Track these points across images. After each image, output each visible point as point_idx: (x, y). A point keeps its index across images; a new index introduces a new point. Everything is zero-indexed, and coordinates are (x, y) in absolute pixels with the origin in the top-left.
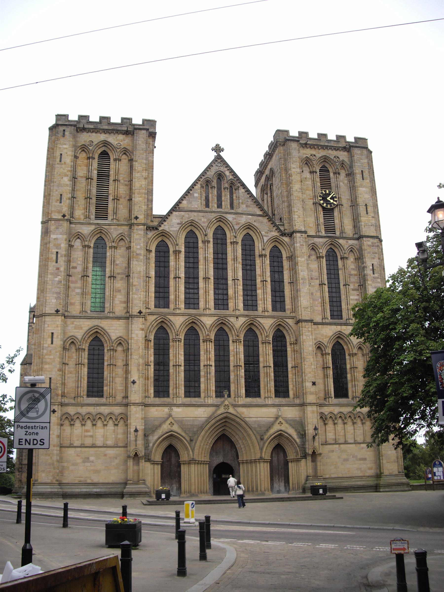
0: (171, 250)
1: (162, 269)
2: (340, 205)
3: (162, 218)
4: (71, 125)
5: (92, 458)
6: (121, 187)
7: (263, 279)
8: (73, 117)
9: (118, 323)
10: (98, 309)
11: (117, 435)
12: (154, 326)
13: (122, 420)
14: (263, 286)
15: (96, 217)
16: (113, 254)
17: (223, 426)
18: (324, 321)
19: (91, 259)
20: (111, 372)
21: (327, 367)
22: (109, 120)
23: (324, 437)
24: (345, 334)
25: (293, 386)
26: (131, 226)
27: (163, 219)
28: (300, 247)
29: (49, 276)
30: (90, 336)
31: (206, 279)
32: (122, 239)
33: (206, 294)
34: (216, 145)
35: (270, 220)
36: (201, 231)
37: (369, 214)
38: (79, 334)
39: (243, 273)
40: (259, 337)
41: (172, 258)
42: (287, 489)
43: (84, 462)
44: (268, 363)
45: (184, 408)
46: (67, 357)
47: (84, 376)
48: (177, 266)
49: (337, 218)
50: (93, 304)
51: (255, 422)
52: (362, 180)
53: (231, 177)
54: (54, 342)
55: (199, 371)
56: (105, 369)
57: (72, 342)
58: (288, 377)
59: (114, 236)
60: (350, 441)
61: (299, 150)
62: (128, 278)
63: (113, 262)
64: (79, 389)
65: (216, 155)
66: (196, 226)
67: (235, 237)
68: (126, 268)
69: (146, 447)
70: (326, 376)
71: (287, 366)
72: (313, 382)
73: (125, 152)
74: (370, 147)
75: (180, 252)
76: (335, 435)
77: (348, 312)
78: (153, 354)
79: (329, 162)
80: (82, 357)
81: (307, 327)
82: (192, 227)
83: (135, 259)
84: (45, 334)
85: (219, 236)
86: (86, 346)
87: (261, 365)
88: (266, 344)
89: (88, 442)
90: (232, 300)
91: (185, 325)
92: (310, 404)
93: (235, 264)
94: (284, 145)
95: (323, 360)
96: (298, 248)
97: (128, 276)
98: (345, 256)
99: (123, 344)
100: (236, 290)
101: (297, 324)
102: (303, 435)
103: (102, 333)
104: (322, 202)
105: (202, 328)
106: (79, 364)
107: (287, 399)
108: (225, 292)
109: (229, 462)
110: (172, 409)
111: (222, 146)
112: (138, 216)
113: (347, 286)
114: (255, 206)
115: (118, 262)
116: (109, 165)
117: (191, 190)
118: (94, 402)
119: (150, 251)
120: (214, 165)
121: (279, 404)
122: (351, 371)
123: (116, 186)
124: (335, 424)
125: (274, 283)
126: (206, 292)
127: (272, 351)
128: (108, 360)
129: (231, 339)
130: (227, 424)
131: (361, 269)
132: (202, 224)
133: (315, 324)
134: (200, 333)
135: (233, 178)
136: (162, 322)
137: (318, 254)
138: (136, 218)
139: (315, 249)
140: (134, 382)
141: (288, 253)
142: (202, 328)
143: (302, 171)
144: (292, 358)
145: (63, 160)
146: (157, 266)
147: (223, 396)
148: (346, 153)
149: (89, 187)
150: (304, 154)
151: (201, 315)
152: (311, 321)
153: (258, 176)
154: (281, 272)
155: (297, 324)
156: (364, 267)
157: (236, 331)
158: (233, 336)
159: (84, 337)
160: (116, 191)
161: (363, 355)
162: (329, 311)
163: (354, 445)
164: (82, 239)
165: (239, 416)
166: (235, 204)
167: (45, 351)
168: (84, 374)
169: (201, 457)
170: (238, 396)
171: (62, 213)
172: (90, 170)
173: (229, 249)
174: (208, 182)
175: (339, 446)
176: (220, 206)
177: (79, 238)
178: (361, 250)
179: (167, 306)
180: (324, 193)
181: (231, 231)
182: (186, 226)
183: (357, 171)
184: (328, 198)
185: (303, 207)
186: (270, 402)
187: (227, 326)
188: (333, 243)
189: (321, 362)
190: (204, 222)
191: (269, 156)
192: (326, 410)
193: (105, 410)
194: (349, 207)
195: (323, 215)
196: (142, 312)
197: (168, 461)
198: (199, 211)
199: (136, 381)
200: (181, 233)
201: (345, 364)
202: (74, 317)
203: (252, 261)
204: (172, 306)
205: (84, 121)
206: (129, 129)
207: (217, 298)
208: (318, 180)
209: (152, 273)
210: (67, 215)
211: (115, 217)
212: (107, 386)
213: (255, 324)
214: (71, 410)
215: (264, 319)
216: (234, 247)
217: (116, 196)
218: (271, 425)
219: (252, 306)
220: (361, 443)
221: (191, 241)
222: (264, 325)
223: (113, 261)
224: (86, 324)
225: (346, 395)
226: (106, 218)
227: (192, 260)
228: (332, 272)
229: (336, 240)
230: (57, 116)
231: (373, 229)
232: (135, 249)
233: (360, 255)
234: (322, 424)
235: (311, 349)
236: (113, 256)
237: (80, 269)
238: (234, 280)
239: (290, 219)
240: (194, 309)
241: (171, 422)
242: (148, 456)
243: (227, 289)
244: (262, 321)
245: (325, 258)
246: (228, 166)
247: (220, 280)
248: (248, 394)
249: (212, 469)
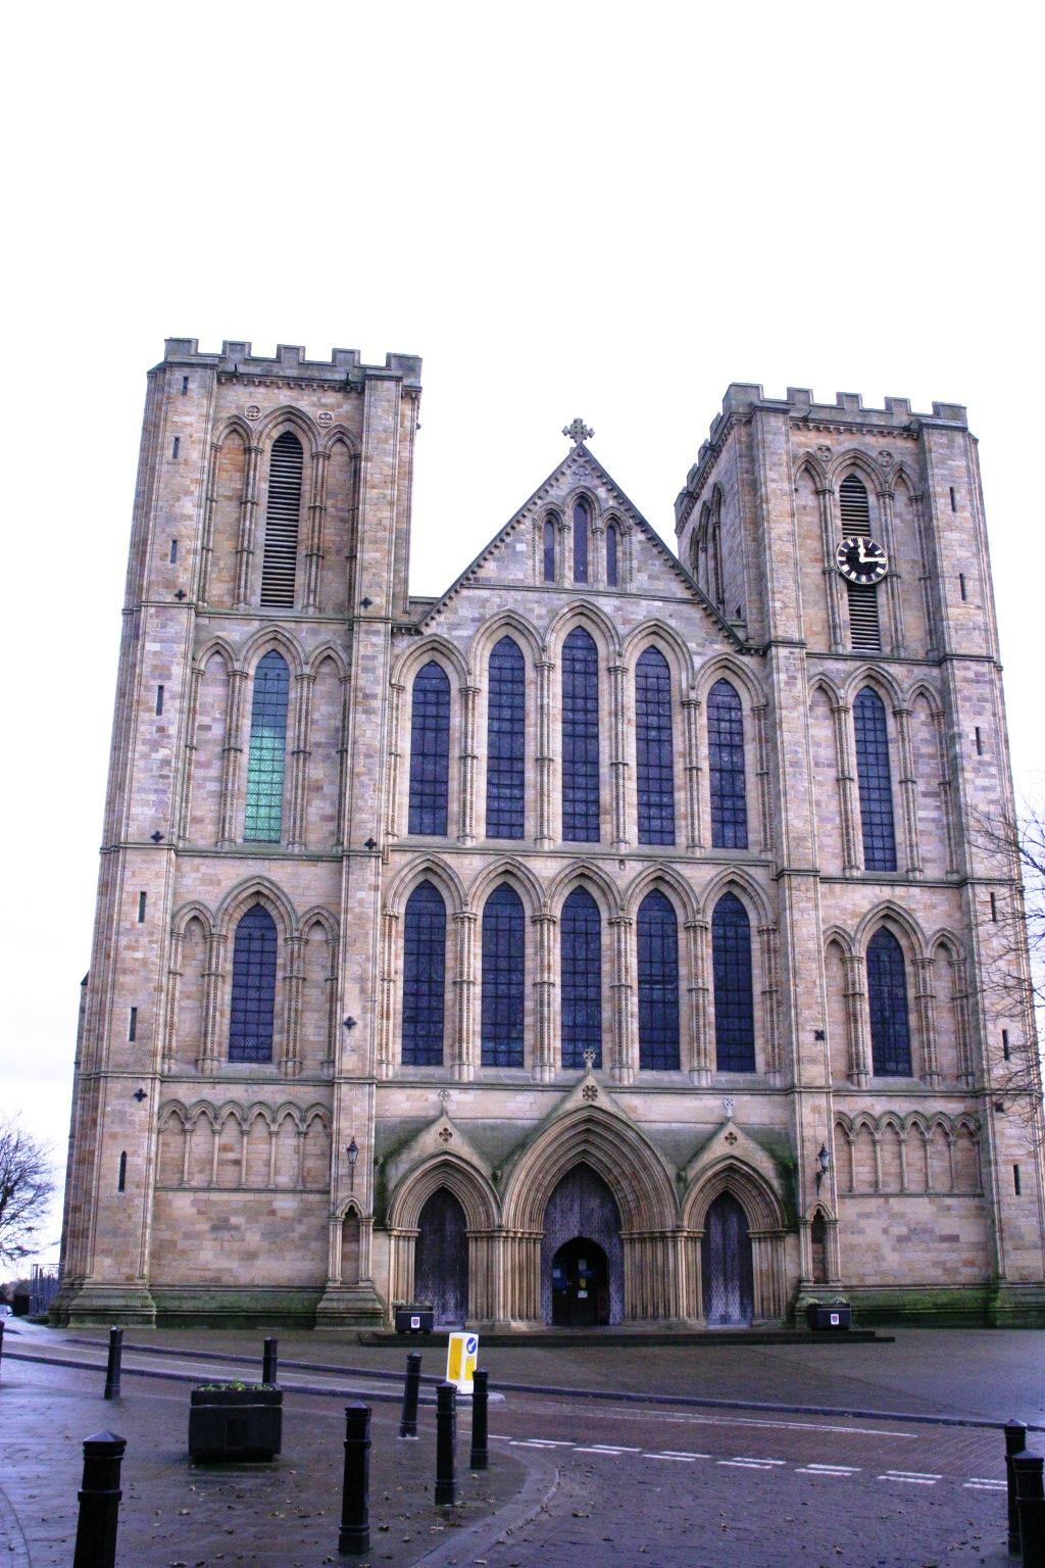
0: (455, 686)
1: (430, 735)
2: (892, 576)
3: (431, 604)
4: (205, 366)
6: (328, 525)
7: (691, 762)
8: (210, 346)
9: (313, 870)
10: (263, 836)
11: (304, 1159)
12: (407, 880)
13: (317, 1120)
14: (691, 781)
15: (262, 601)
16: (305, 694)
17: (579, 1144)
18: (848, 875)
19: (249, 707)
20: (294, 996)
21: (854, 995)
22: (301, 353)
23: (845, 1177)
24: (900, 907)
25: (767, 1042)
26: (350, 624)
27: (433, 607)
28: (787, 684)
29: (141, 748)
30: (241, 903)
31: (542, 761)
32: (329, 657)
33: (542, 800)
34: (575, 422)
35: (709, 612)
36: (530, 638)
37: (969, 599)
38: (211, 898)
39: (638, 748)
40: (680, 912)
41: (456, 709)
42: (749, 1315)
43: (215, 1228)
44: (700, 981)
45: (480, 1092)
46: (180, 957)
47: (222, 1005)
48: (470, 728)
49: (886, 609)
50: (250, 823)
51: (666, 1132)
52: (950, 512)
53: (612, 503)
54: (147, 917)
55: (521, 998)
56: (277, 989)
57: (195, 918)
58: (751, 1017)
59: (309, 649)
60: (913, 1188)
61: (787, 436)
62: (342, 758)
63: (305, 716)
64: (209, 1039)
65: (575, 445)
66: (520, 627)
67: (620, 655)
68: (337, 730)
69: (382, 1195)
70: (851, 1017)
71: (750, 989)
72: (817, 1032)
73: (342, 436)
75: (477, 691)
76: (876, 1172)
77: (911, 851)
78: (401, 952)
79: (865, 467)
80: (218, 957)
81: (803, 888)
82: (510, 628)
83: (360, 709)
84: (124, 896)
85: (580, 654)
86: (229, 929)
87: (683, 986)
88: (695, 932)
89: (229, 1175)
90: (608, 817)
91: (486, 881)
92: (813, 1090)
93: (620, 725)
94: (749, 422)
95: (846, 975)
96: (782, 685)
97: (343, 752)
98: (905, 706)
99: (326, 925)
100: (621, 791)
101: (777, 880)
102: (788, 1170)
103: (272, 896)
104: (846, 568)
105: (529, 886)
106: (209, 975)
107: (749, 1076)
108: (592, 797)
109: (595, 1237)
110: (449, 1095)
111: (589, 424)
112: (372, 599)
113: (910, 784)
114: (673, 576)
115: (316, 715)
116: (300, 468)
117: (508, 534)
118: (246, 1075)
119: (401, 689)
120: (568, 472)
121: (725, 1087)
122: (918, 1005)
123: (317, 523)
124: (874, 1143)
125: (718, 775)
126: (542, 794)
127: (710, 951)
128: (285, 966)
129: (604, 915)
130: (592, 1138)
131: (947, 739)
132: (535, 622)
133: (825, 880)
134: (525, 899)
135: (616, 505)
136: (427, 869)
137: (834, 700)
138: (366, 603)
139: (827, 688)
140: (350, 1024)
141: (755, 699)
142: (529, 886)
143: (796, 490)
144: (762, 968)
145: (181, 453)
146: (419, 730)
147: (583, 1065)
148: (910, 444)
149: (248, 523)
150: (800, 445)
151: (527, 854)
152: (814, 873)
153: (683, 507)
154: (737, 748)
155: (777, 880)
156: (953, 737)
157: (617, 896)
158: (610, 908)
159: (225, 906)
160: (316, 534)
161: (950, 964)
162: (861, 849)
163: (926, 1200)
164: (225, 655)
165: (623, 1116)
167: (123, 941)
168: (223, 999)
169: (522, 1226)
170: (620, 1064)
171: (175, 587)
172: (251, 480)
173: (604, 685)
174: (553, 517)
175: (887, 1202)
176: (581, 575)
177: (218, 652)
178: (945, 691)
179: (440, 829)
180: (852, 545)
181: (610, 640)
182: (495, 626)
183: (939, 488)
184: (863, 559)
185: (796, 582)
186: (705, 1081)
187: (595, 882)
188: (873, 673)
189: (840, 982)
190: (540, 617)
191: (710, 452)
193: (272, 1094)
194: (917, 582)
195: (847, 603)
196: (375, 844)
197: (435, 1232)
198: (528, 589)
199: (356, 1019)
200: (481, 643)
201: (904, 986)
202: (202, 854)
203: (662, 718)
204: (453, 829)
205: (237, 356)
206: (350, 378)
207: (570, 810)
208: (837, 512)
209: (405, 745)
210: (188, 592)
211: (311, 602)
212: (281, 1032)
213: (668, 878)
214: (186, 1094)
215: (690, 866)
216: (616, 681)
217: (315, 547)
218: (703, 1143)
219: (662, 832)
220: (944, 1195)
221: (508, 665)
222: (691, 881)
223: (304, 711)
224: (232, 874)
226: (291, 604)
227: (507, 713)
228: (871, 748)
229: (882, 665)
230: (169, 341)
231: (977, 636)
232: (361, 683)
233: (943, 701)
234: (842, 1141)
235: (812, 945)
236: (304, 699)
237: (218, 730)
238: (616, 764)
239: (763, 613)
240: (511, 837)
241: (446, 1130)
242: (383, 1218)
243: (597, 789)
244: (685, 871)
245: (851, 712)
246: (602, 474)
247: (577, 766)
248: (648, 1061)
249: (552, 1256)
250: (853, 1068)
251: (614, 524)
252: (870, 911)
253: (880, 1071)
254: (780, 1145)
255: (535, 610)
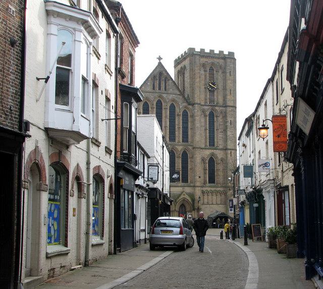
70: (205, 173)
74: (235, 57)
102: (193, 200)
166: (167, 89)
174: (155, 77)
176: (160, 89)
186: (180, 185)
192: (204, 189)
208: (208, 75)
218: (180, 195)
225: (214, 182)
239: (193, 97)
250: (205, 183)
251: (166, 78)
254: (192, 196)
255: (151, 97)
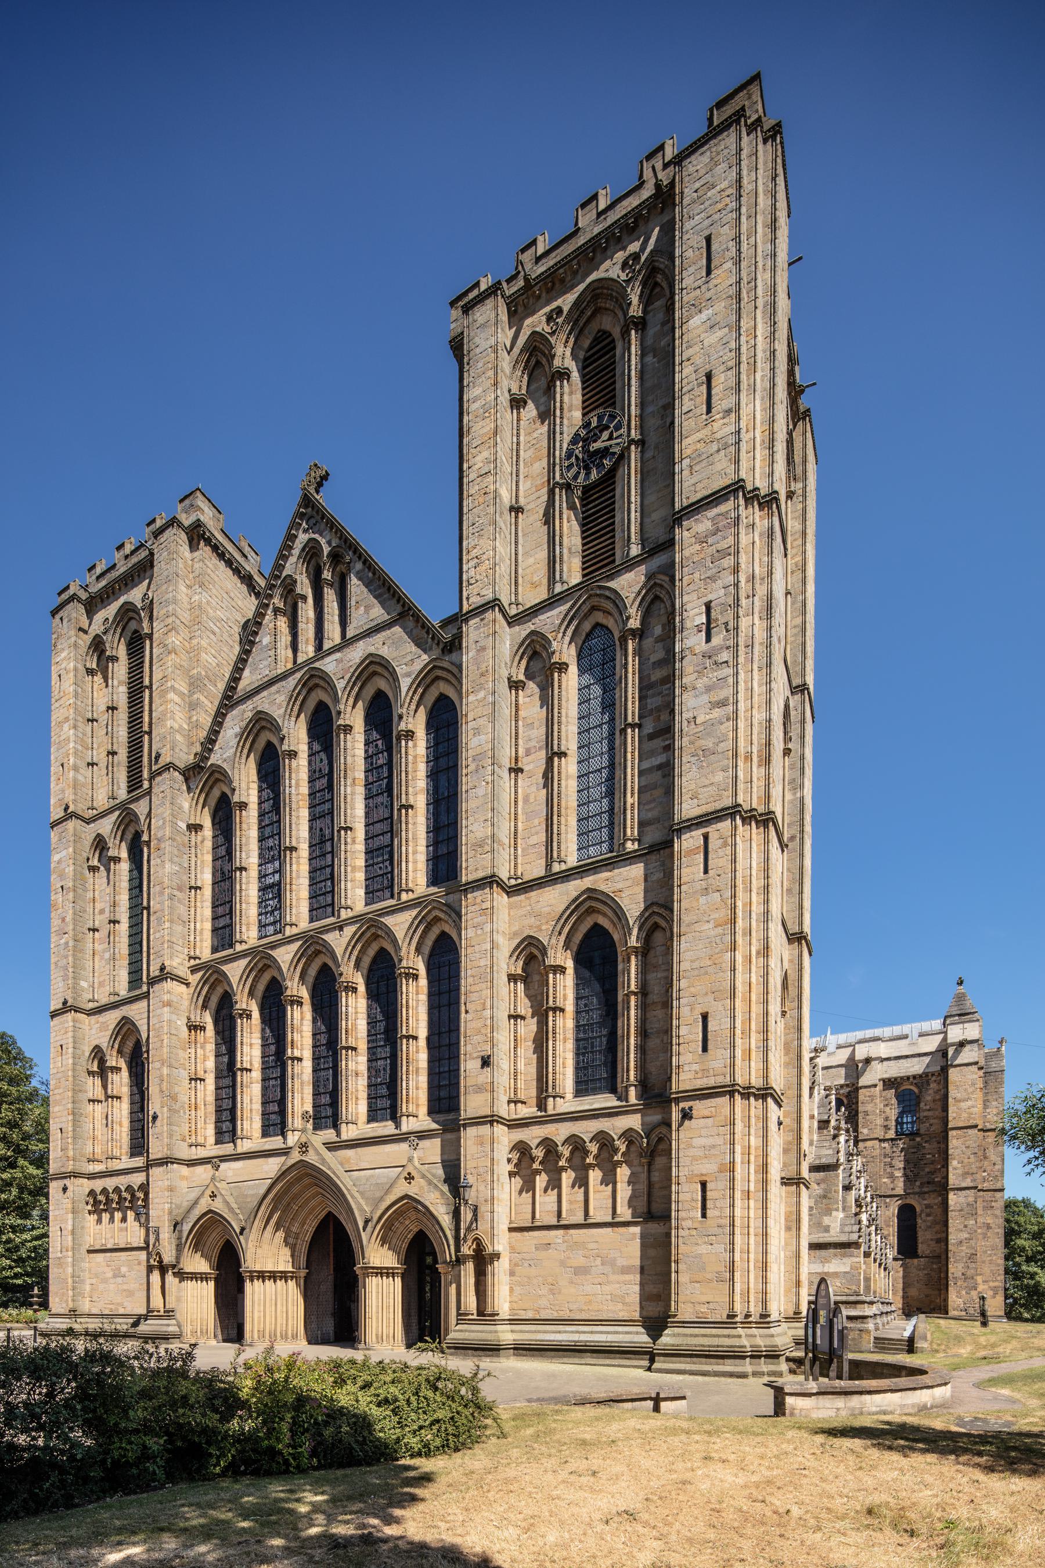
5: (124, 1269)
43: (115, 1276)
252: (567, 908)
253: (582, 1088)
